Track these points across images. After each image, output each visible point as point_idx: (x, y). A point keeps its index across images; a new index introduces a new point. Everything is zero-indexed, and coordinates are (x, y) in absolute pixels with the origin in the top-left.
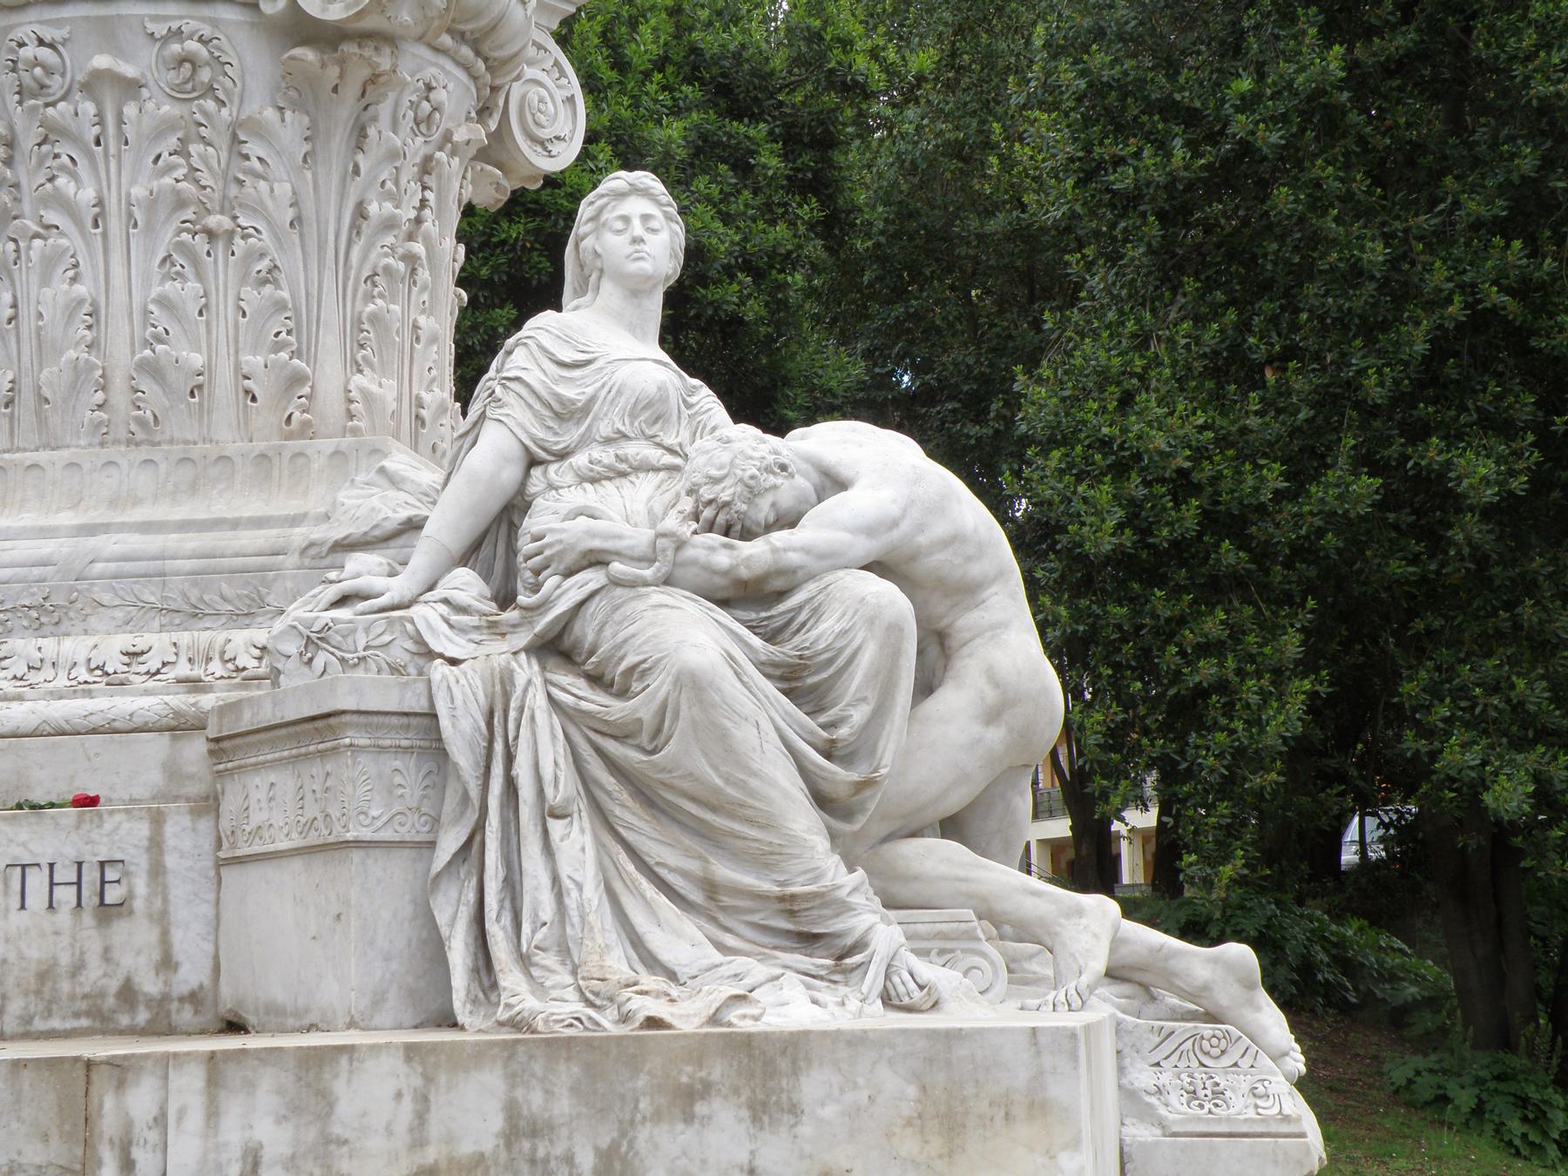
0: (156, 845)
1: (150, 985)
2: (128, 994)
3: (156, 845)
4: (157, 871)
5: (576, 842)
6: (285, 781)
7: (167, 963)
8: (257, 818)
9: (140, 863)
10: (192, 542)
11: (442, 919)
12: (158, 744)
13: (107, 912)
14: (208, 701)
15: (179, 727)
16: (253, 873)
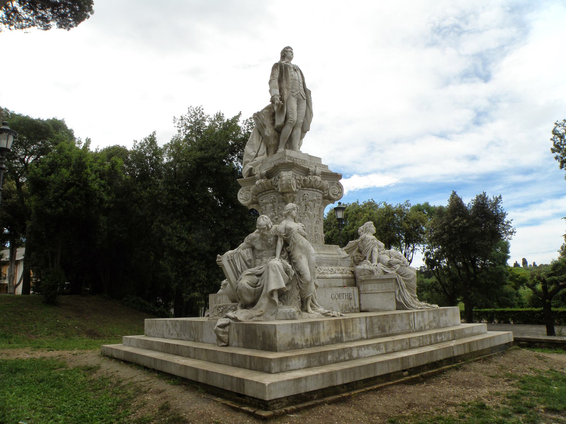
0: (353, 292)
1: (354, 307)
2: (352, 308)
3: (353, 292)
4: (354, 294)
5: (406, 290)
6: (377, 285)
7: (355, 305)
8: (369, 289)
9: (352, 293)
10: (330, 256)
11: (398, 299)
12: (341, 280)
13: (350, 299)
14: (345, 275)
15: (344, 278)
16: (369, 295)
